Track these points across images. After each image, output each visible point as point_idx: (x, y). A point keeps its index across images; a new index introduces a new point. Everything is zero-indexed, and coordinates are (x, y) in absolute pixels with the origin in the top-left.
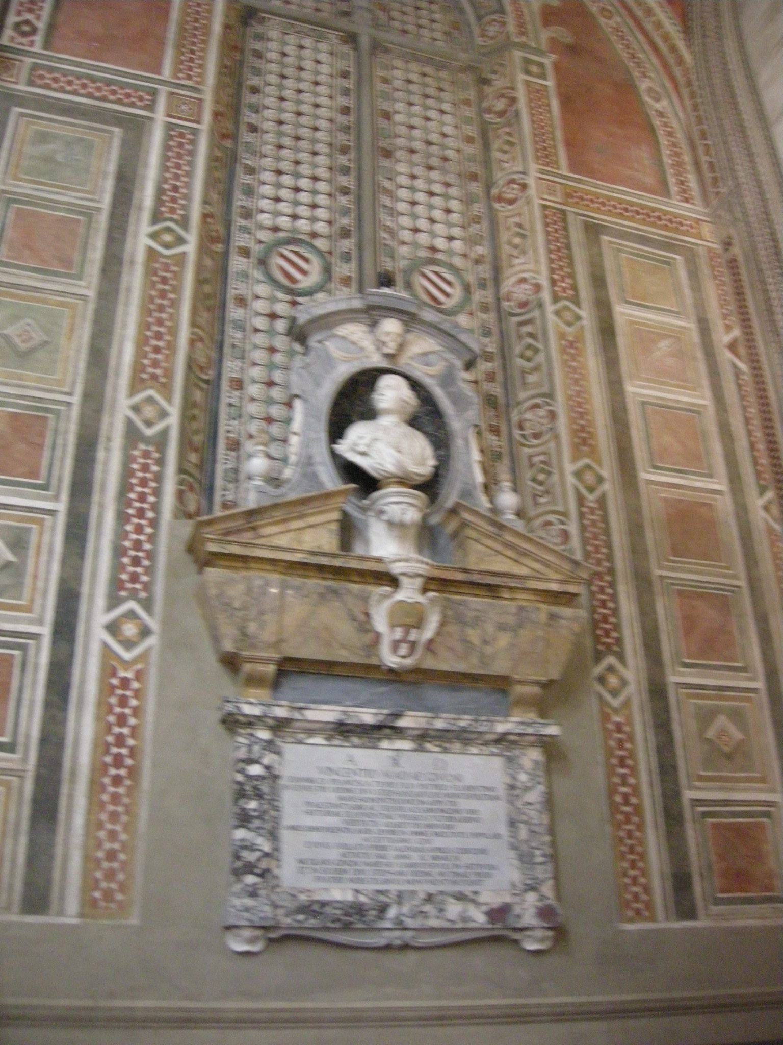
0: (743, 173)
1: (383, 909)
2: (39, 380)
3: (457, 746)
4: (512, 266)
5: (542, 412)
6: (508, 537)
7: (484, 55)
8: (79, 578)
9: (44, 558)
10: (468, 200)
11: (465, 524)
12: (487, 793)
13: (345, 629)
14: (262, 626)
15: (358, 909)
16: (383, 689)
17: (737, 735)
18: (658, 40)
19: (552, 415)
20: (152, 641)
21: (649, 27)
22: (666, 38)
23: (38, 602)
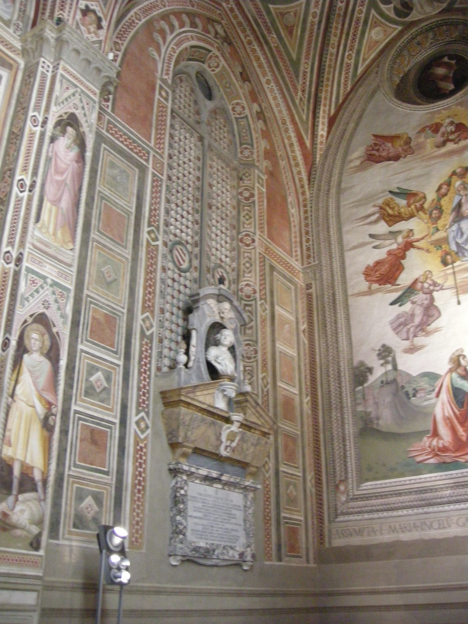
0: (325, 261)
1: (214, 551)
2: (113, 298)
3: (232, 488)
4: (244, 277)
5: (252, 348)
6: (258, 409)
7: (243, 164)
8: (127, 399)
9: (116, 387)
10: (232, 239)
11: (247, 401)
12: (236, 507)
13: (213, 438)
14: (192, 434)
15: (207, 551)
16: (215, 463)
17: (295, 493)
18: (297, 179)
19: (256, 352)
20: (149, 431)
21: (295, 171)
22: (301, 180)
23: (115, 407)
